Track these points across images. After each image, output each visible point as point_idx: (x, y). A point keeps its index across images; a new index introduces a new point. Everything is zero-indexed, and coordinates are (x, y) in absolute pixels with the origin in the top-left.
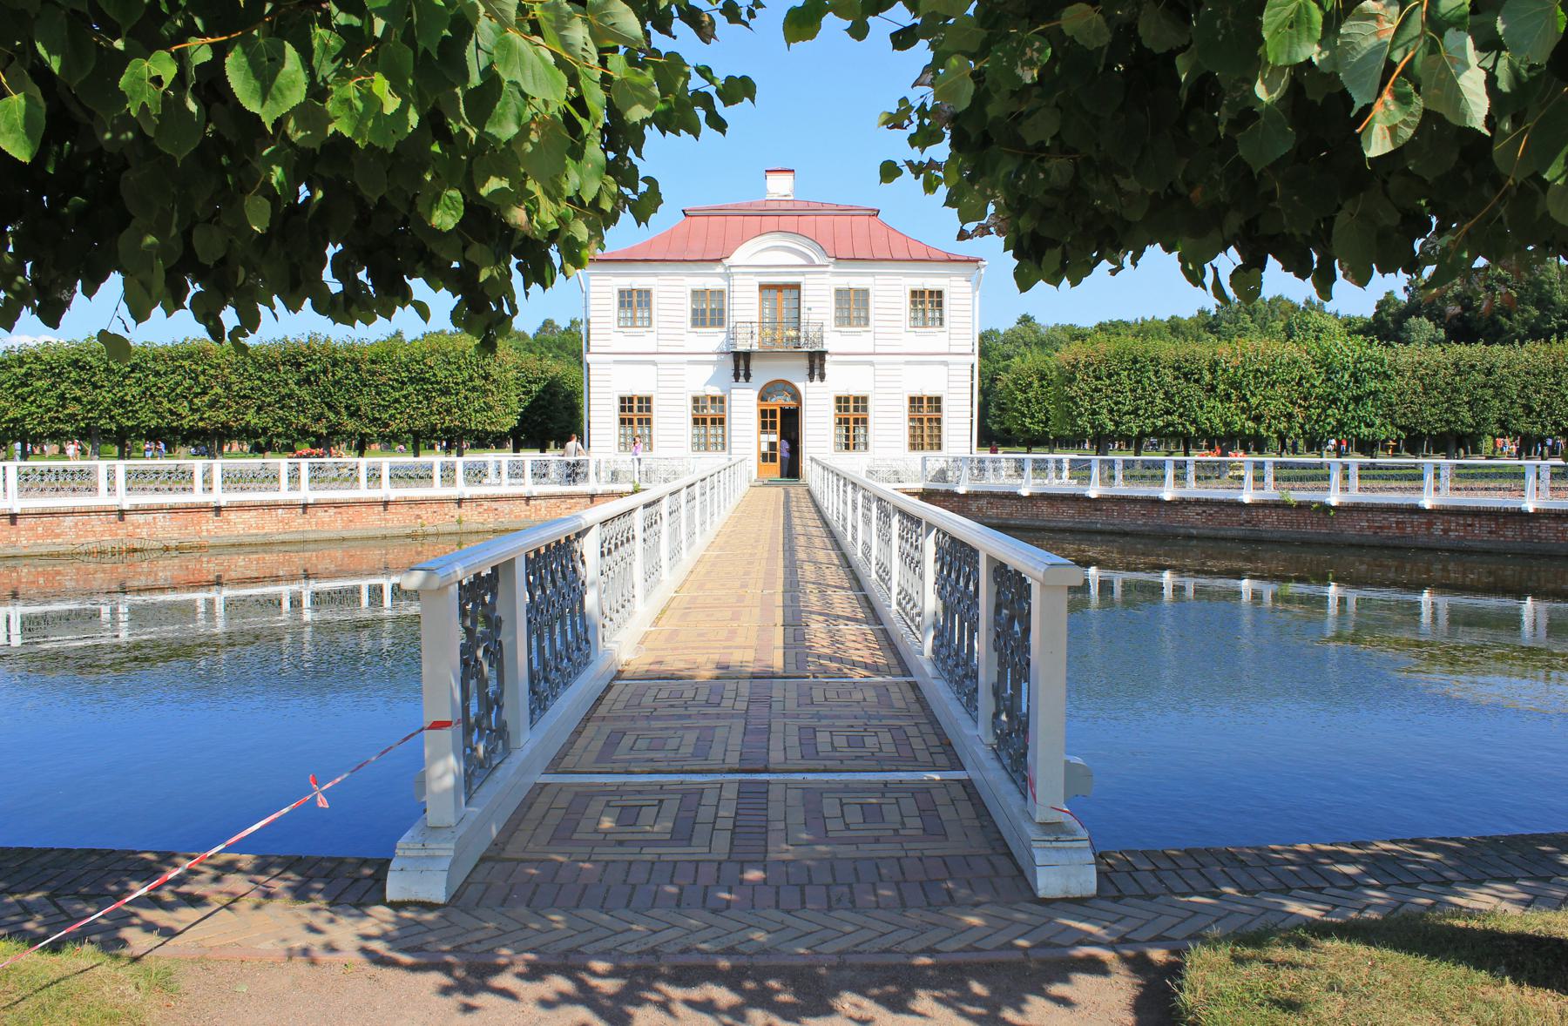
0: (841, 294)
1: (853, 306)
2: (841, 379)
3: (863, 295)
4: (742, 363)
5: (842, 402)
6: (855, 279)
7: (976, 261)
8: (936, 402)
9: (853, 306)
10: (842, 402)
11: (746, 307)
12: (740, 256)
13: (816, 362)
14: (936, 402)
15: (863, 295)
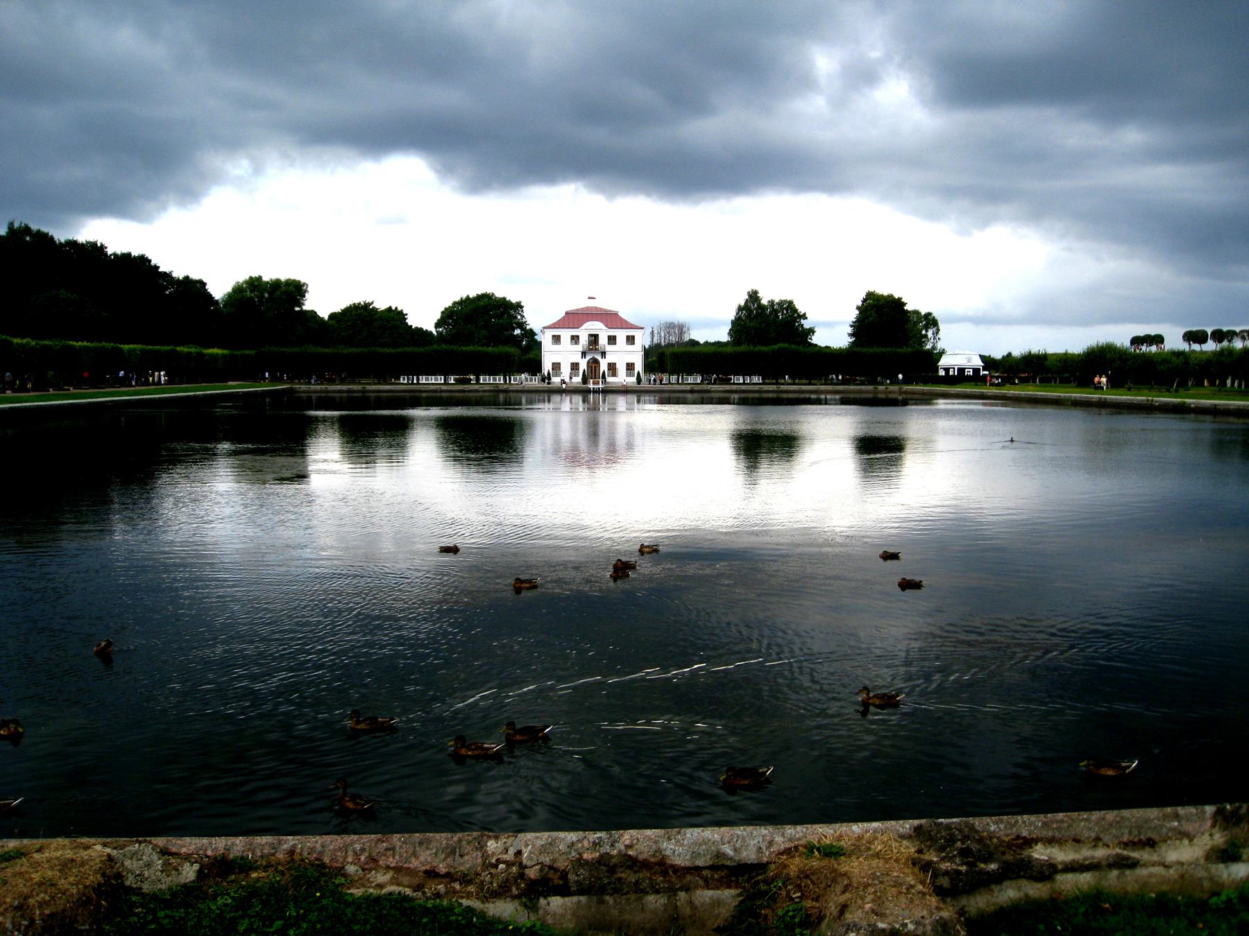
0: (610, 338)
1: (612, 340)
2: (610, 358)
3: (614, 338)
4: (584, 354)
5: (610, 365)
6: (612, 332)
7: (642, 328)
8: (633, 364)
9: (612, 340)
10: (610, 365)
11: (584, 340)
12: (584, 327)
13: (603, 354)
14: (633, 364)
15: (614, 338)
